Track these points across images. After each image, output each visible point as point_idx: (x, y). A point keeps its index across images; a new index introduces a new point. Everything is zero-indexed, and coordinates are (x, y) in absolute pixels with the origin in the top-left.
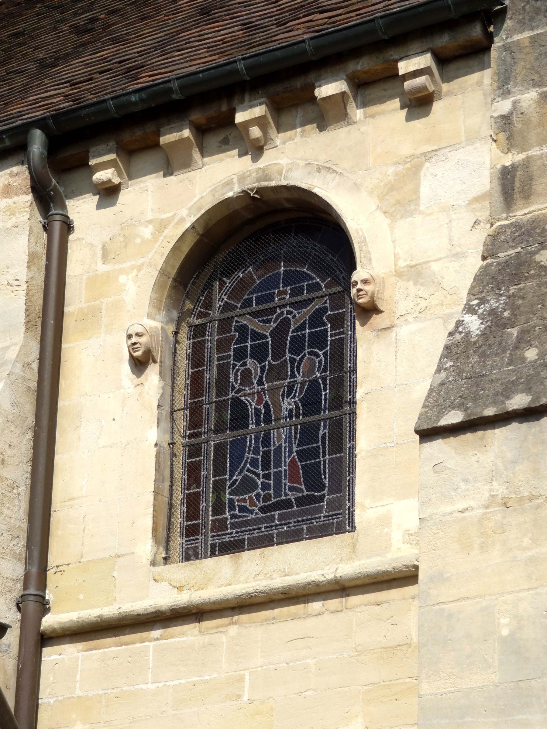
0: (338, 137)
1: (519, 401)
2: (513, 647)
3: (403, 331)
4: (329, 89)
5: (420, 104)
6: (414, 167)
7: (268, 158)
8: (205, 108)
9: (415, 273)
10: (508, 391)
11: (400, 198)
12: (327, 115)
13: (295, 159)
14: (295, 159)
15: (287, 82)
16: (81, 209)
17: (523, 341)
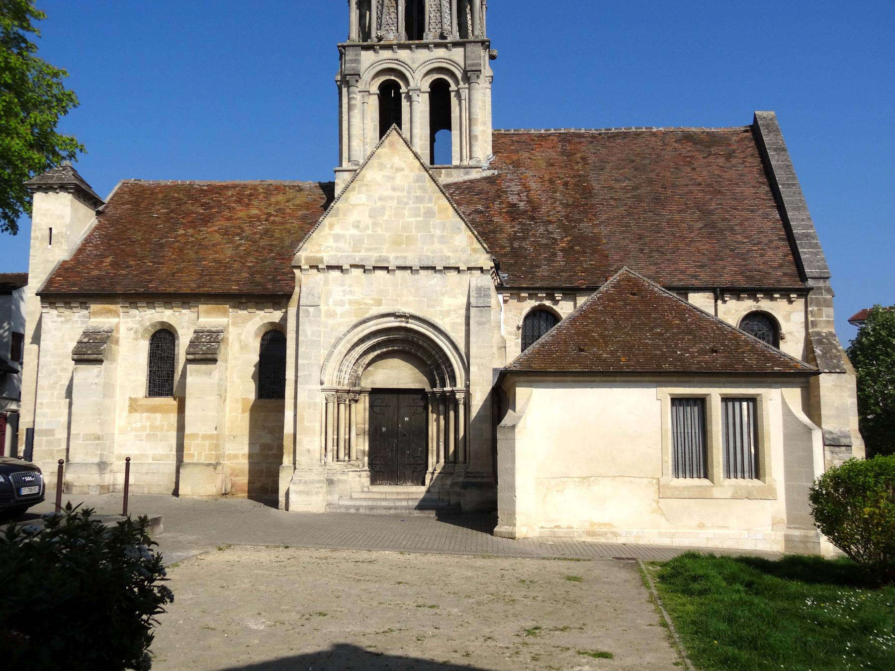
0: (773, 303)
1: (838, 370)
2: (837, 408)
3: (789, 343)
4: (776, 296)
5: (790, 302)
6: (790, 313)
7: (759, 304)
8: (752, 293)
9: (791, 333)
10: (834, 368)
11: (787, 318)
12: (772, 299)
13: (765, 305)
14: (765, 305)
15: (769, 293)
16: (720, 302)
17: (831, 358)
